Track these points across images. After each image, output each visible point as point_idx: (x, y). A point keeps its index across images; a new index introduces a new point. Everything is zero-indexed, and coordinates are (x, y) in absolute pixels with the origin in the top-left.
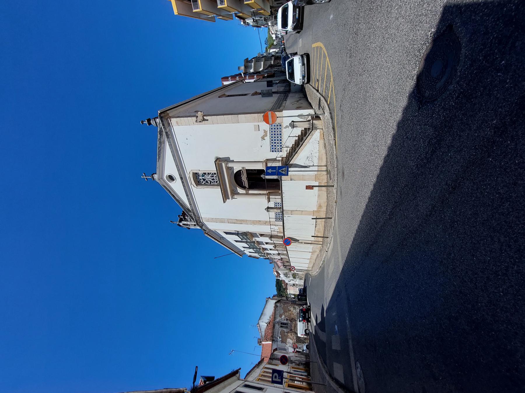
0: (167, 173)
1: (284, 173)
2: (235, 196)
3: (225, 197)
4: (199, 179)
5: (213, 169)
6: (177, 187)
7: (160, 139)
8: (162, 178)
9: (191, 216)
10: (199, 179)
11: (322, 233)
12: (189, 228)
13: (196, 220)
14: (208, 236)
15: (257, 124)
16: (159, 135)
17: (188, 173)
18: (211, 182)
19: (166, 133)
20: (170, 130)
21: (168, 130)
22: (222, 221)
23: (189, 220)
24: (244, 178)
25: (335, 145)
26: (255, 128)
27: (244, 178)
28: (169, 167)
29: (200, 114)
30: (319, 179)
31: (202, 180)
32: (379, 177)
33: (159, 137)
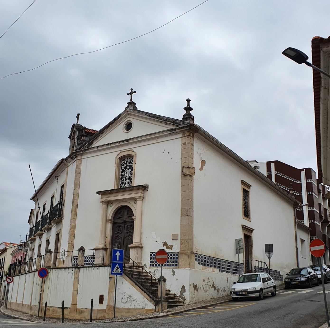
1: (115, 269)
4: (126, 163)
10: (126, 163)
22: (77, 185)
30: (109, 309)
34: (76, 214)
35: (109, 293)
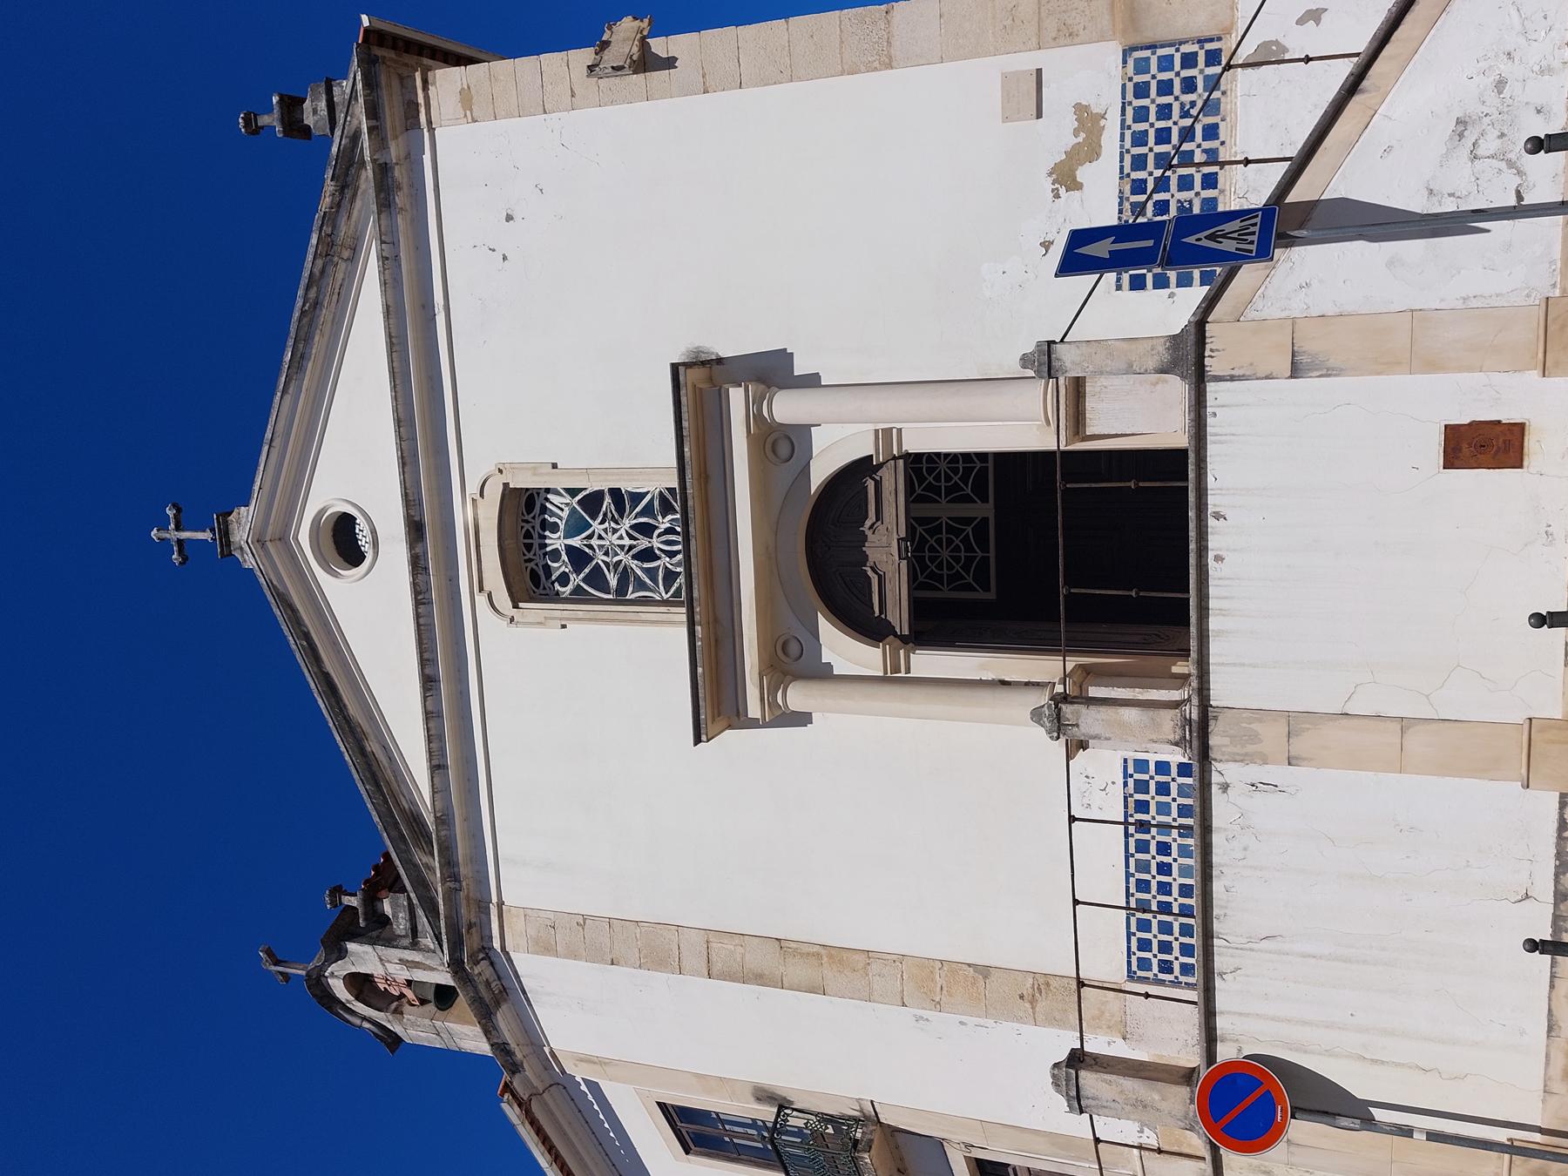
0: (327, 493)
1: (1229, 246)
2: (797, 697)
3: (716, 704)
4: (545, 546)
5: (647, 455)
6: (371, 618)
9: (422, 885)
10: (545, 546)
12: (394, 1041)
15: (1026, 61)
16: (329, 187)
17: (472, 488)
18: (625, 576)
19: (383, 170)
21: (395, 151)
22: (652, 948)
23: (401, 925)
24: (884, 547)
26: (1007, 96)
27: (884, 547)
28: (351, 456)
29: (625, 33)
31: (561, 566)
33: (325, 202)
34: (836, 956)
35: (1433, 365)
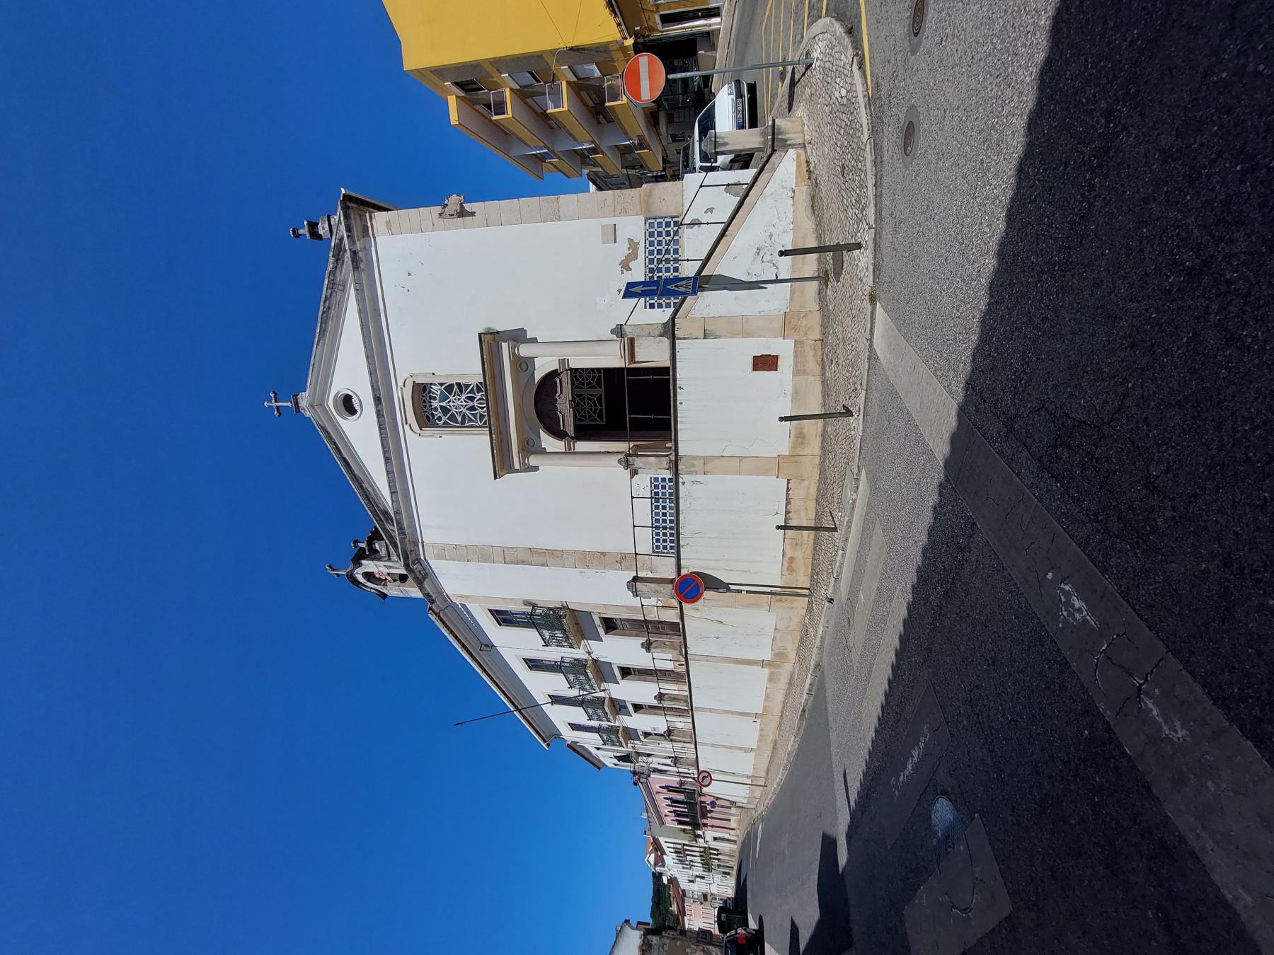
0: (339, 386)
1: (682, 289)
2: (533, 461)
3: (502, 464)
4: (430, 406)
5: (470, 369)
6: (361, 434)
7: (333, 273)
8: (321, 405)
9: (390, 537)
10: (430, 406)
11: (812, 514)
12: (384, 596)
13: (405, 552)
14: (439, 624)
15: (611, 221)
16: (331, 260)
17: (400, 383)
18: (464, 416)
19: (354, 253)
20: (367, 250)
21: (359, 245)
22: (484, 555)
23: (383, 553)
24: (564, 404)
25: (861, 66)
26: (603, 234)
27: (564, 404)
28: (348, 370)
29: (454, 201)
30: (795, 329)
31: (438, 414)
32: (1003, 288)
33: (330, 266)
34: (552, 553)
35: (749, 335)
